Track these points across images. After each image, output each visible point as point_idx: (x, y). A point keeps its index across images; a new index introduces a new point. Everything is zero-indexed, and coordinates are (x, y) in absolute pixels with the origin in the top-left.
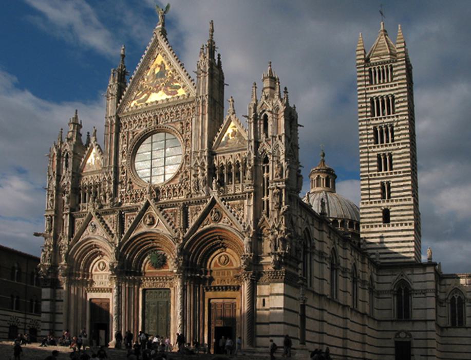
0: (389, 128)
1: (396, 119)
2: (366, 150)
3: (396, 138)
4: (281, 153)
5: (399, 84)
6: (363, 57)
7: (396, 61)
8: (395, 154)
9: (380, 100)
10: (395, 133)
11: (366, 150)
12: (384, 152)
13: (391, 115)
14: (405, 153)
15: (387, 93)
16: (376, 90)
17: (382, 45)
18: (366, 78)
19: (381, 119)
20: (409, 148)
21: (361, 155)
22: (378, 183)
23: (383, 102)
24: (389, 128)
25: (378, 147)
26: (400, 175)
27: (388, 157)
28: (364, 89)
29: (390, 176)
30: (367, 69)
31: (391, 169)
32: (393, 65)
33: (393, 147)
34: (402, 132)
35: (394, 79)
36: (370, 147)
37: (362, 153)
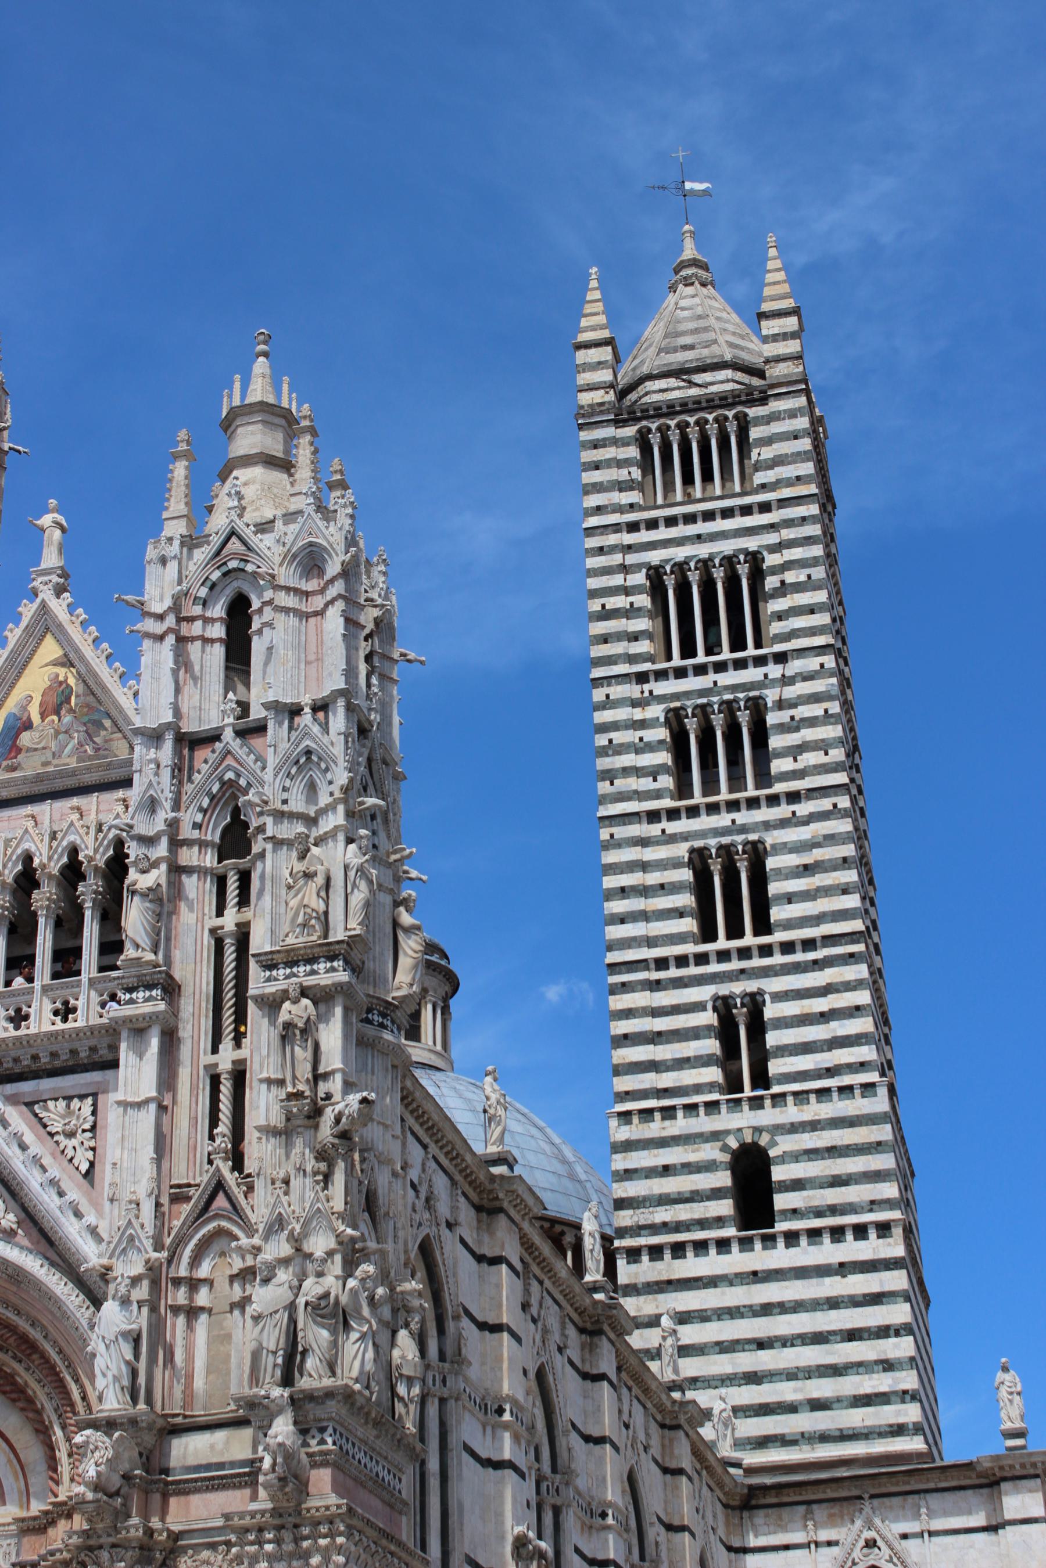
0: (744, 718)
1: (774, 671)
3: (778, 766)
4: (324, 800)
5: (783, 503)
6: (605, 376)
7: (763, 400)
9: (694, 577)
10: (775, 742)
12: (726, 840)
13: (751, 651)
14: (831, 839)
15: (727, 547)
17: (691, 325)
18: (625, 471)
19: (701, 670)
20: (845, 814)
21: (611, 857)
22: (698, 1007)
23: (708, 587)
24: (744, 718)
25: (693, 812)
26: (811, 956)
27: (743, 867)
28: (616, 528)
29: (757, 962)
30: (630, 431)
31: (763, 926)
32: (752, 412)
33: (765, 814)
35: (759, 478)
36: (653, 816)
37: (613, 843)
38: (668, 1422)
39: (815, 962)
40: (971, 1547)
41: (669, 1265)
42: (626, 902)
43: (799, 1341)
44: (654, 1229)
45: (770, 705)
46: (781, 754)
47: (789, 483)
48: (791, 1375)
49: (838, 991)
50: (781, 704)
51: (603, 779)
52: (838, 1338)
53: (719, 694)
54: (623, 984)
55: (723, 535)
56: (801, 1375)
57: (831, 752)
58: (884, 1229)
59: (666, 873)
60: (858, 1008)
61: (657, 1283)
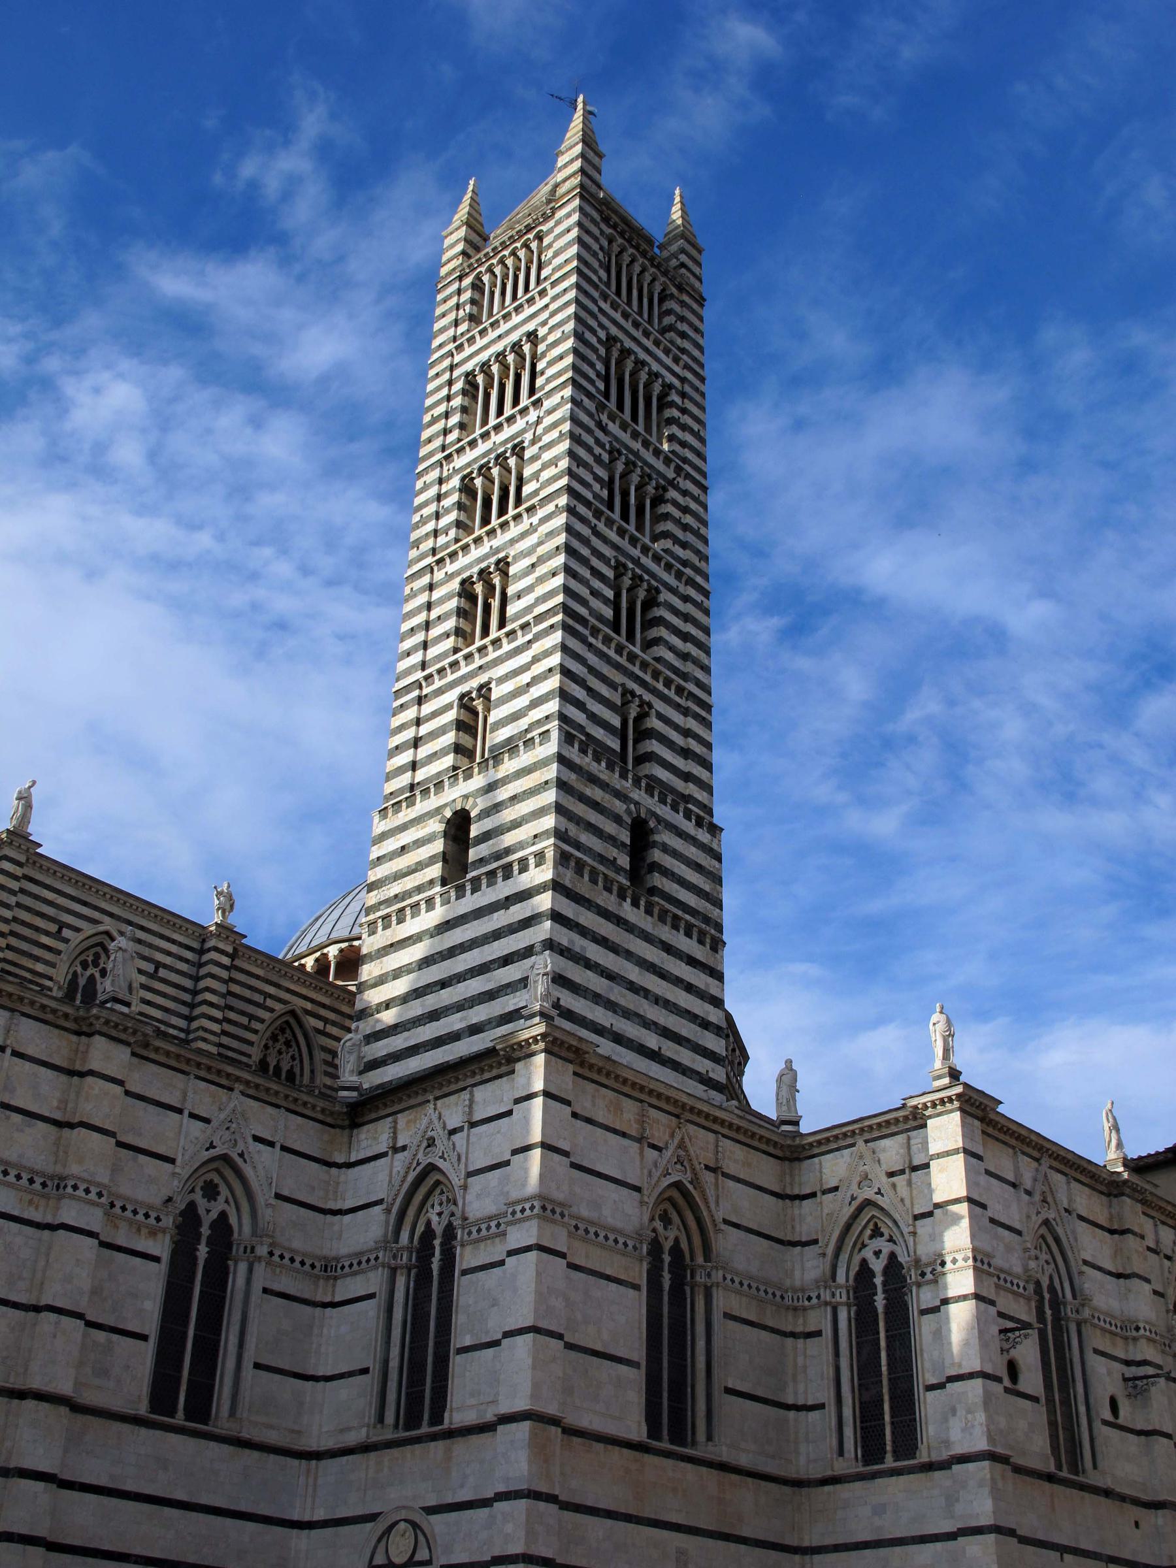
2: (426, 580)
8: (517, 558)
11: (426, 580)
12: (483, 565)
16: (486, 340)
29: (492, 655)
30: (467, 281)
32: (544, 228)
34: (547, 456)
37: (414, 595)
38: (85, 1029)
39: (529, 642)
40: (498, 1132)
41: (394, 930)
42: (413, 638)
43: (469, 976)
44: (387, 902)
45: (525, 445)
46: (530, 481)
47: (560, 267)
48: (460, 1007)
49: (539, 660)
50: (533, 442)
51: (413, 548)
52: (496, 965)
53: (496, 450)
54: (402, 705)
55: (515, 327)
56: (466, 1006)
57: (560, 464)
58: (540, 857)
59: (443, 606)
60: (550, 670)
61: (384, 948)
